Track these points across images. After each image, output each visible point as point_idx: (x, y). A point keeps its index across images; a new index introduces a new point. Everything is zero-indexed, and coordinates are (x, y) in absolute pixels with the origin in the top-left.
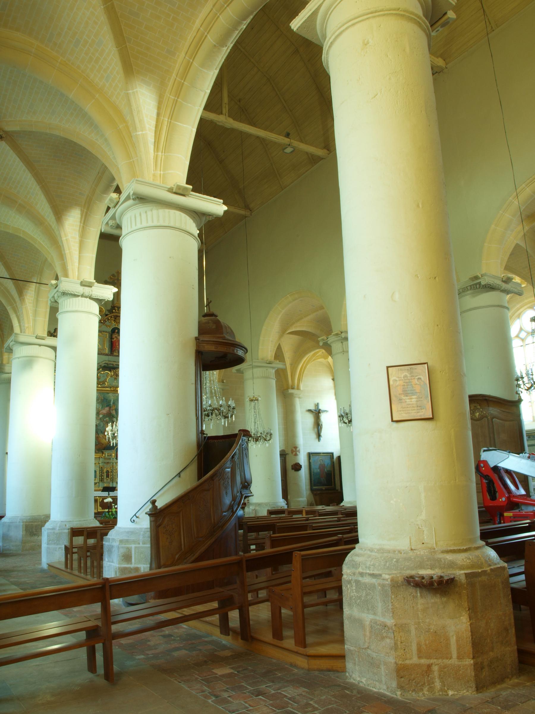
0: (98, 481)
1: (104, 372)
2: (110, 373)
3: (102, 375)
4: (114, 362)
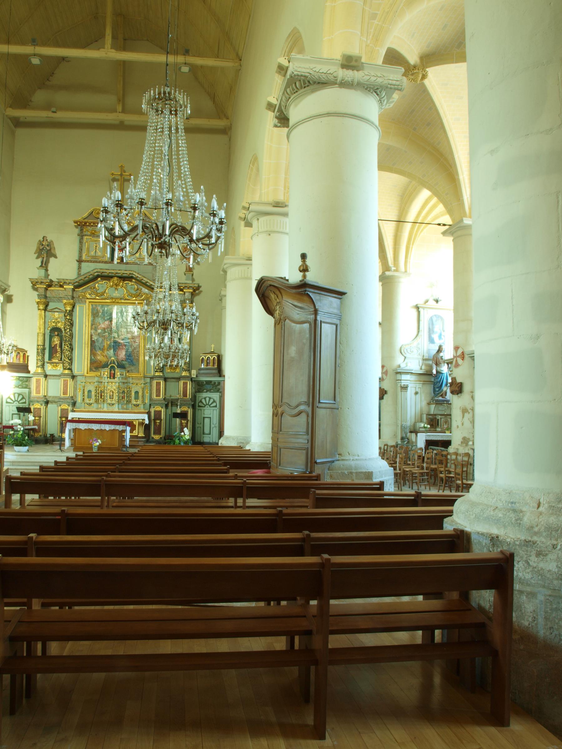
0: (93, 401)
1: (102, 281)
2: (109, 283)
3: (99, 285)
4: (107, 269)
